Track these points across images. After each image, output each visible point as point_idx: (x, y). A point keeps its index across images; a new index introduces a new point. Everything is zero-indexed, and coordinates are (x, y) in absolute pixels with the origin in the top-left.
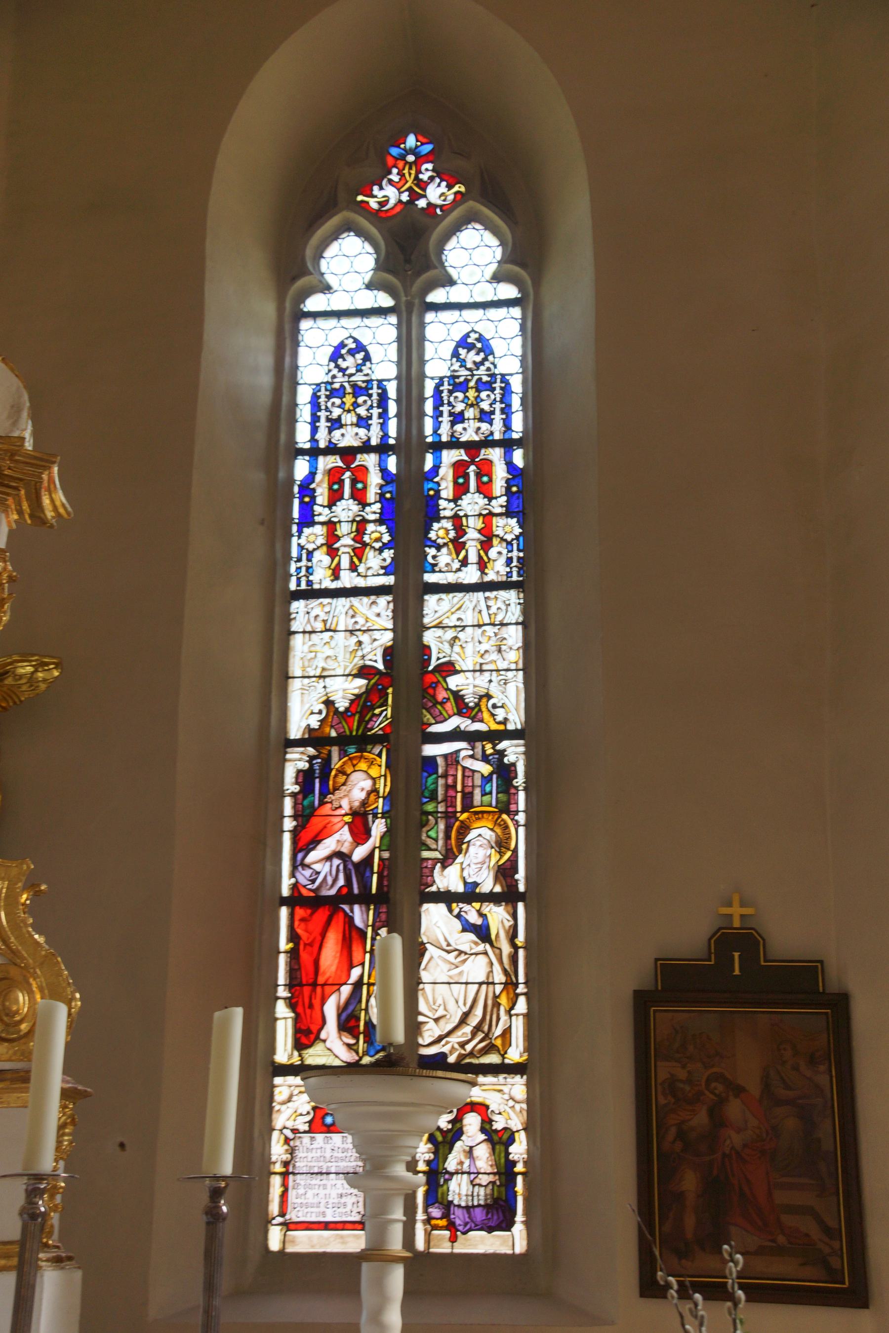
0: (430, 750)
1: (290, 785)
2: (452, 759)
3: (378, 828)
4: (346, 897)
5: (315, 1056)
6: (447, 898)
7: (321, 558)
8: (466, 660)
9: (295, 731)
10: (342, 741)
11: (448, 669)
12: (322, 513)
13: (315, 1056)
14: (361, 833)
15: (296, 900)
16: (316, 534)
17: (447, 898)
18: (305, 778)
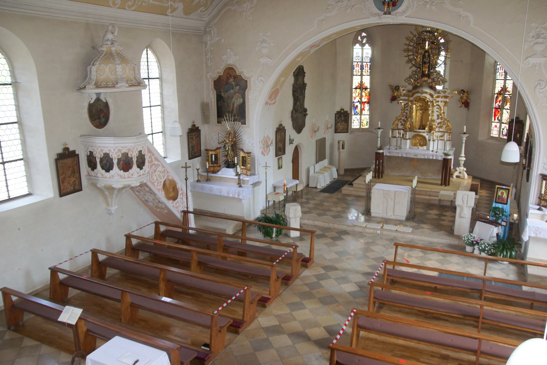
0: (506, 95)
1: (495, 98)
2: (507, 97)
3: (501, 102)
4: (498, 108)
5: (495, 121)
6: (506, 109)
7: (499, 76)
8: (509, 87)
9: (496, 93)
10: (499, 94)
11: (507, 88)
12: (499, 71)
13: (495, 121)
14: (500, 103)
15: (495, 108)
16: (499, 73)
17: (506, 109)
18: (496, 97)
